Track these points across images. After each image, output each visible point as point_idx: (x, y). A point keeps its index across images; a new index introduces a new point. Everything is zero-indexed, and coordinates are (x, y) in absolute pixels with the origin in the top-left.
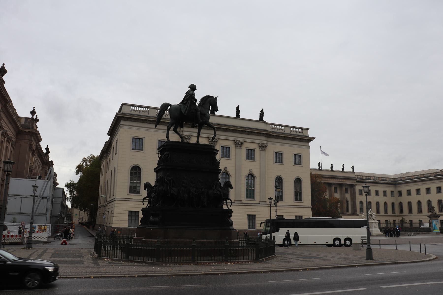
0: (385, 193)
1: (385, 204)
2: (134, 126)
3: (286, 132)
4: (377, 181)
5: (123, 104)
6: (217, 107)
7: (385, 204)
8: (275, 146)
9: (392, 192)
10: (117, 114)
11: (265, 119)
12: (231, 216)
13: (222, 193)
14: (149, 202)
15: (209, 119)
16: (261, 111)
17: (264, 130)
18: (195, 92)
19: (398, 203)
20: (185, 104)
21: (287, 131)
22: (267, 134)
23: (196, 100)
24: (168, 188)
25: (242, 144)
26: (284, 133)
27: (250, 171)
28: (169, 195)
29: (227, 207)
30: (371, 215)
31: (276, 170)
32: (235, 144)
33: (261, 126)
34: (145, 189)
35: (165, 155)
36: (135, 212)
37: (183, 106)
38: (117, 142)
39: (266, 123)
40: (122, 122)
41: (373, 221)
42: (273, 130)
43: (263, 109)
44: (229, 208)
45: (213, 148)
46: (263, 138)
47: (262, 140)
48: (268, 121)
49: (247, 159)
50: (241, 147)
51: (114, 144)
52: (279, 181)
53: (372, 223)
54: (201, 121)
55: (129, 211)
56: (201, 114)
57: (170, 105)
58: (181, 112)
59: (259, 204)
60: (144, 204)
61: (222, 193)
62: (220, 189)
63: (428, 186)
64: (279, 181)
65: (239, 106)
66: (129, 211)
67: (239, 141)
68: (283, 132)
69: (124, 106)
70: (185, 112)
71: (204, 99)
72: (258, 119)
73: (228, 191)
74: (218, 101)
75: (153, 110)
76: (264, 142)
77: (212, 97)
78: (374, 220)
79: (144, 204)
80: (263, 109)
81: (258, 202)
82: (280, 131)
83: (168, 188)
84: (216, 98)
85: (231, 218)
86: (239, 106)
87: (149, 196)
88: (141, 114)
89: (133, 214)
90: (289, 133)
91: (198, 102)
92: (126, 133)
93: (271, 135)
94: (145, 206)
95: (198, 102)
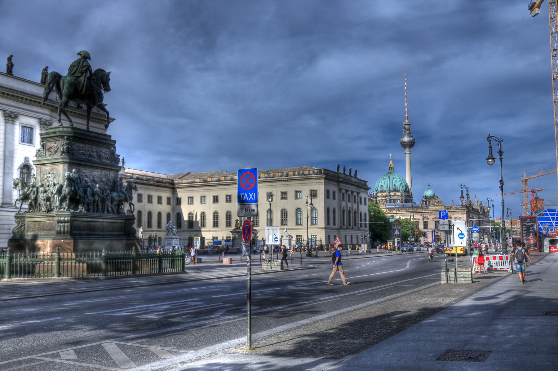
0: (160, 199)
1: (160, 214)
4: (151, 182)
6: (109, 86)
7: (160, 214)
9: (169, 199)
13: (127, 196)
16: (44, 70)
19: (175, 213)
22: (52, 106)
24: (77, 188)
27: (26, 159)
30: (171, 229)
32: (6, 117)
41: (174, 237)
43: (47, 67)
49: (22, 141)
50: (13, 122)
53: (173, 238)
63: (216, 193)
65: (12, 56)
67: (12, 112)
73: (131, 194)
74: (110, 77)
76: (47, 118)
78: (174, 235)
80: (47, 67)
83: (77, 188)
86: (12, 56)
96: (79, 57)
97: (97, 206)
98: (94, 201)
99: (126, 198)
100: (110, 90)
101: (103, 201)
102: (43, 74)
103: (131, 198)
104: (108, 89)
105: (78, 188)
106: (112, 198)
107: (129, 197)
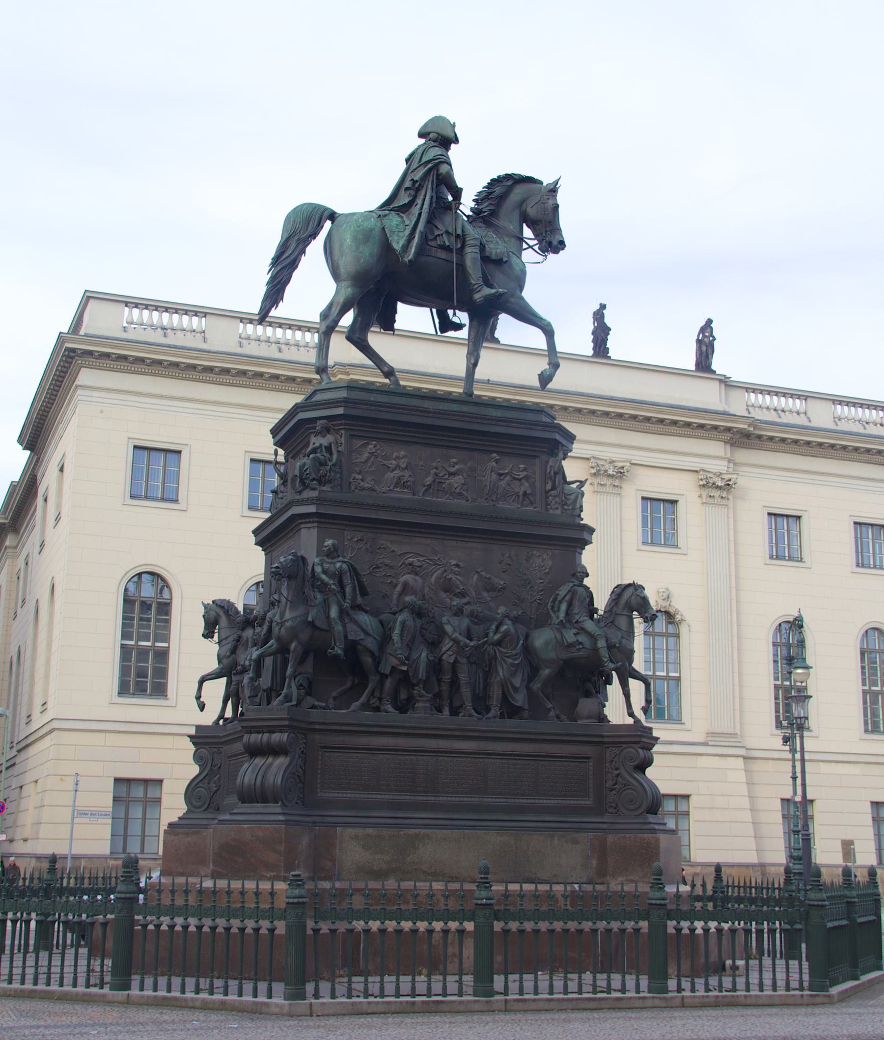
2: (136, 393)
3: (815, 423)
5: (88, 298)
8: (770, 484)
10: (61, 339)
11: (718, 364)
12: (649, 762)
13: (601, 644)
14: (232, 694)
15: (521, 287)
16: (702, 330)
17: (716, 413)
18: (454, 153)
20: (404, 209)
21: (822, 417)
22: (729, 429)
23: (457, 193)
25: (621, 474)
26: (807, 428)
28: (339, 650)
29: (631, 714)
31: (777, 590)
33: (703, 395)
34: (208, 634)
35: (314, 451)
36: (146, 782)
37: (394, 220)
38: (62, 470)
39: (725, 382)
40: (86, 376)
42: (758, 415)
43: (709, 322)
44: (637, 721)
45: (545, 419)
46: (717, 448)
47: (712, 455)
48: (736, 376)
51: (48, 480)
52: (791, 645)
54: (487, 291)
55: (117, 780)
56: (486, 259)
57: (332, 216)
58: (386, 246)
59: (705, 744)
60: (202, 707)
61: (601, 644)
62: (589, 625)
64: (791, 645)
65: (603, 307)
66: (117, 780)
68: (801, 421)
69: (92, 303)
70: (406, 247)
71: (498, 190)
72: (689, 363)
74: (561, 198)
75: (224, 323)
76: (720, 466)
77: (530, 180)
79: (202, 707)
80: (709, 322)
81: (700, 738)
82: (787, 419)
83: (334, 613)
84: (553, 190)
85: (650, 772)
86: (603, 307)
87: (228, 669)
88: (172, 340)
89: (138, 792)
90: (831, 425)
91: (467, 205)
92: (104, 423)
93: (747, 435)
94: (208, 718)
95: (467, 205)
96: (423, 141)
97: (454, 683)
98: (436, 667)
99: (596, 650)
100: (562, 245)
101: (484, 664)
102: (699, 342)
103: (629, 655)
104: (551, 242)
105: (342, 612)
106: (527, 650)
107: (610, 647)
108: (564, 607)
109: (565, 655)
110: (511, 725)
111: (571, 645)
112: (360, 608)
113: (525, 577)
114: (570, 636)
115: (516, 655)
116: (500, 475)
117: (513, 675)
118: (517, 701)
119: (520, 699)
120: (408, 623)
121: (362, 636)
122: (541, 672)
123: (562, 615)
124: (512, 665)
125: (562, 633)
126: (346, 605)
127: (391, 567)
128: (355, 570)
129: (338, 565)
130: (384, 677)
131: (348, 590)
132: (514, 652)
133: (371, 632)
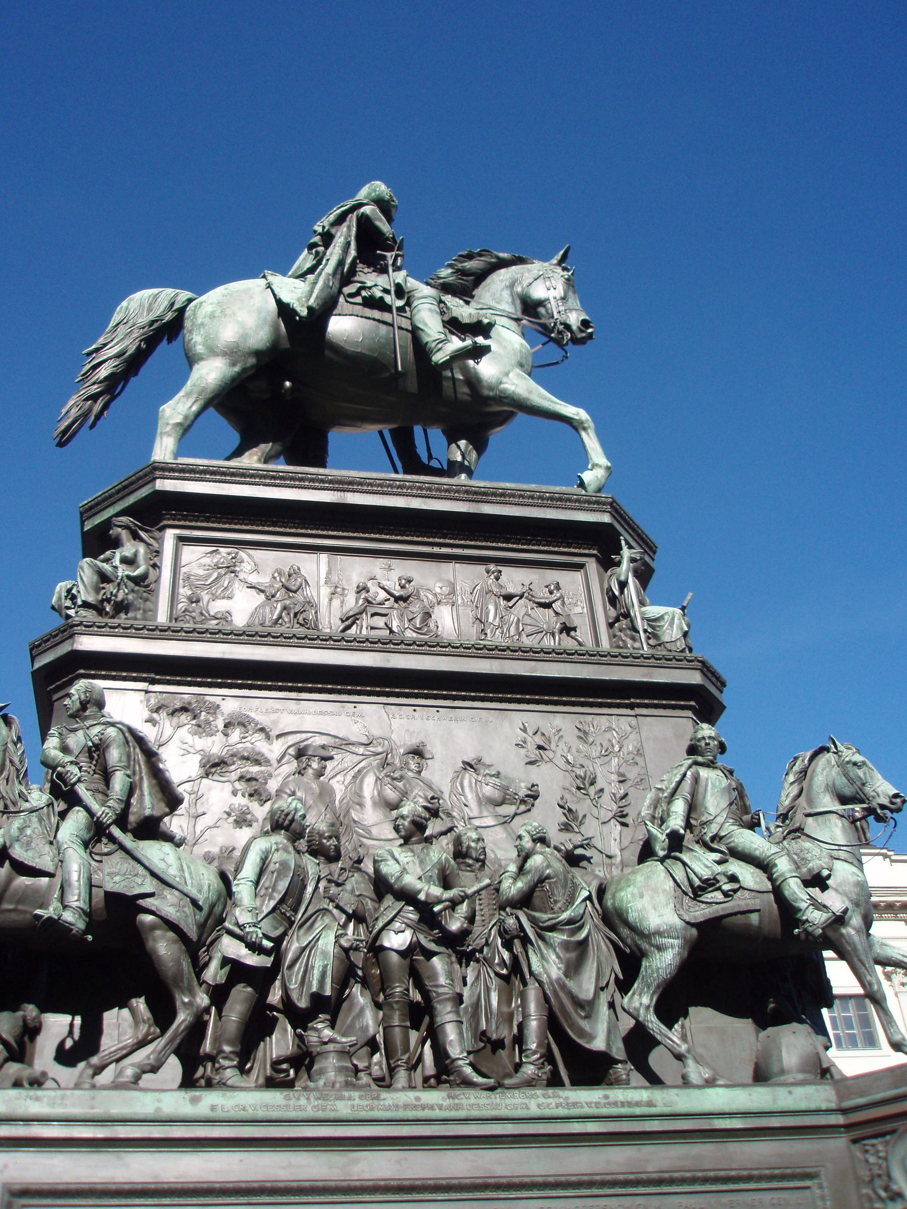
108: (679, 807)
109: (700, 913)
110: (587, 1098)
111: (709, 884)
112: (150, 829)
113: (581, 772)
114: (702, 863)
115: (570, 922)
116: (508, 597)
117: (573, 968)
118: (591, 1037)
119: (601, 1034)
120: (276, 857)
121: (149, 886)
122: (644, 963)
123: (676, 822)
124: (566, 946)
125: (684, 864)
126: (105, 812)
127: (257, 762)
128: (140, 741)
129: (96, 730)
130: (219, 995)
131: (119, 782)
132: (564, 916)
133: (176, 881)
